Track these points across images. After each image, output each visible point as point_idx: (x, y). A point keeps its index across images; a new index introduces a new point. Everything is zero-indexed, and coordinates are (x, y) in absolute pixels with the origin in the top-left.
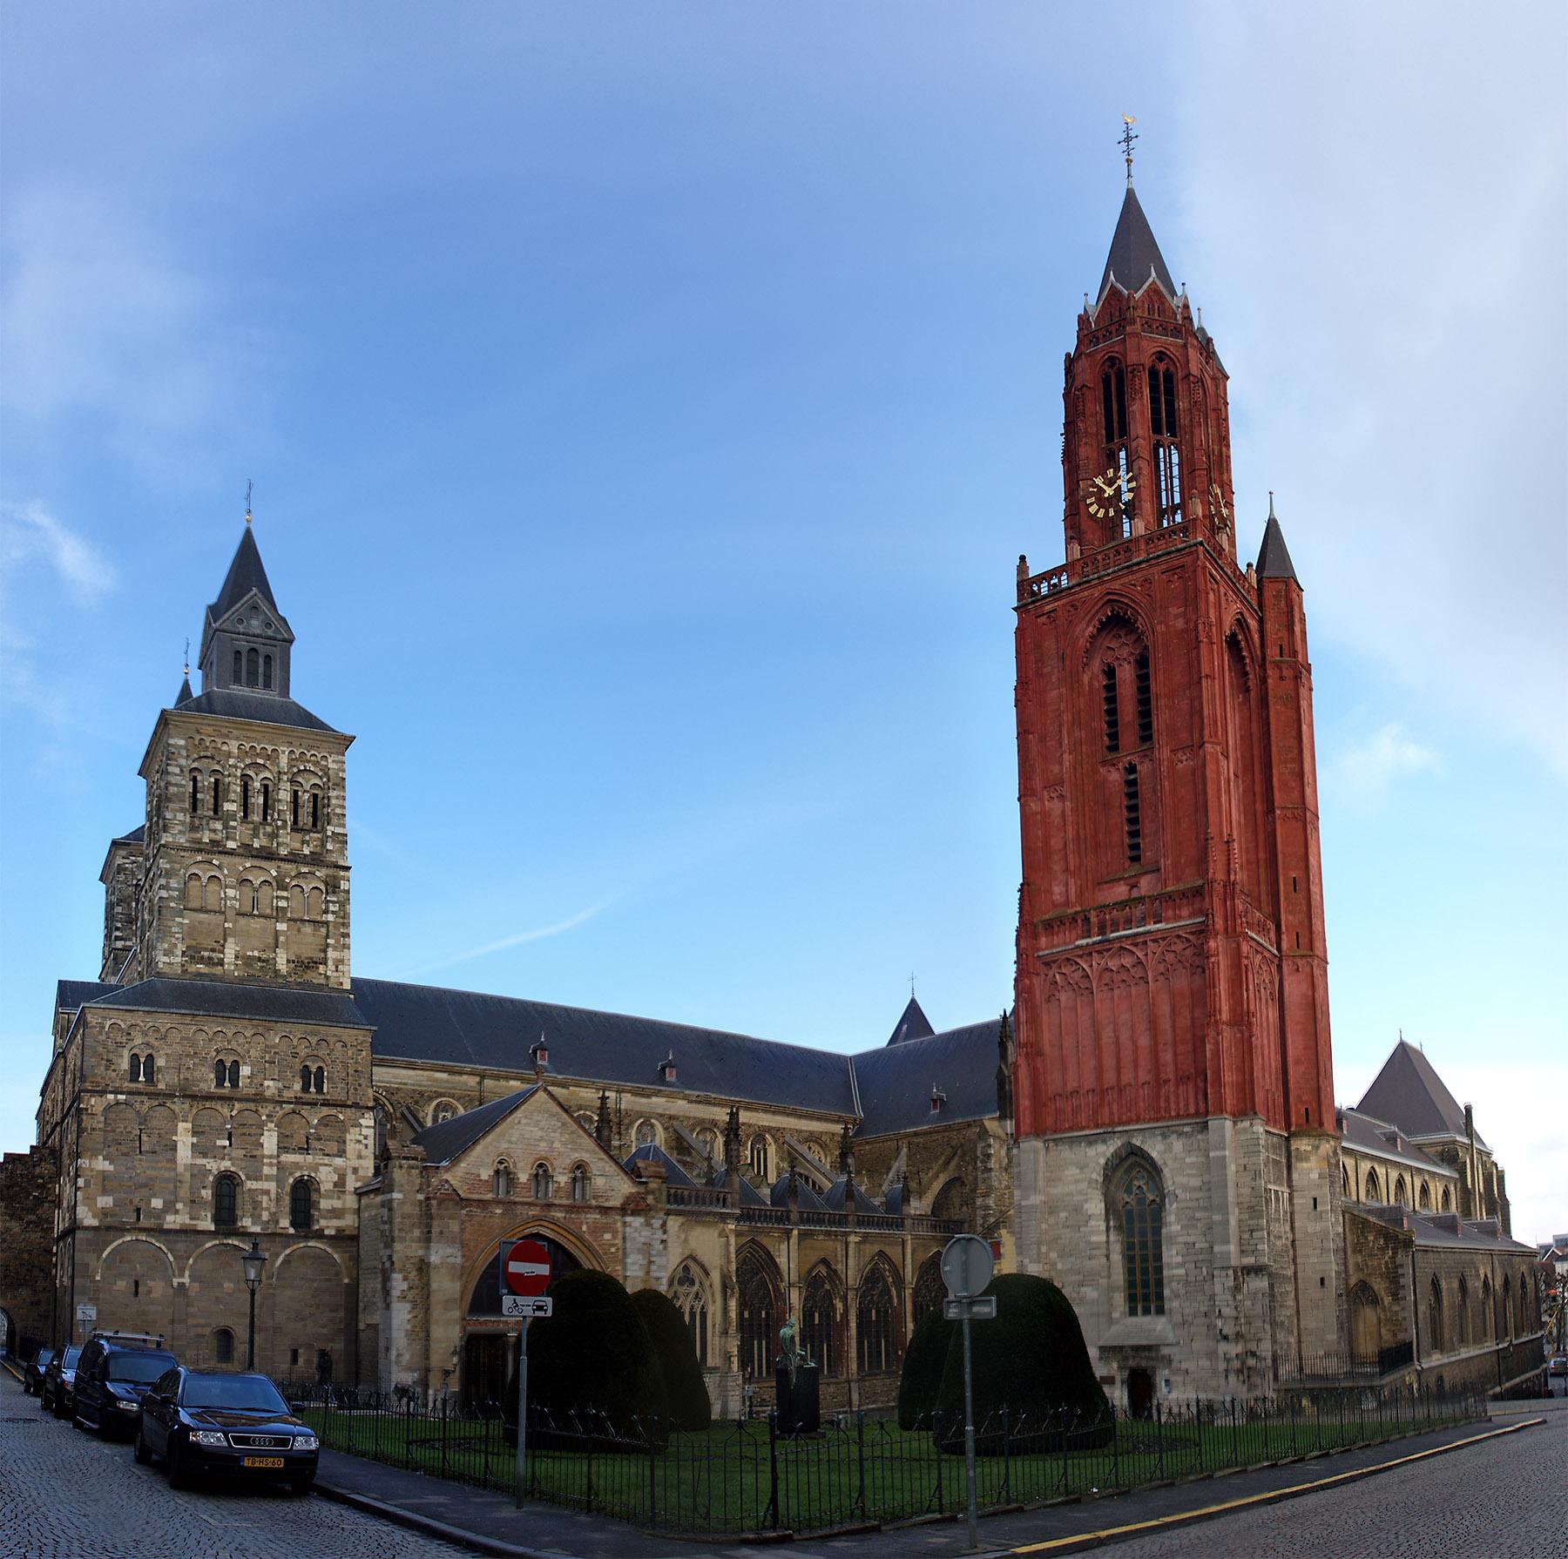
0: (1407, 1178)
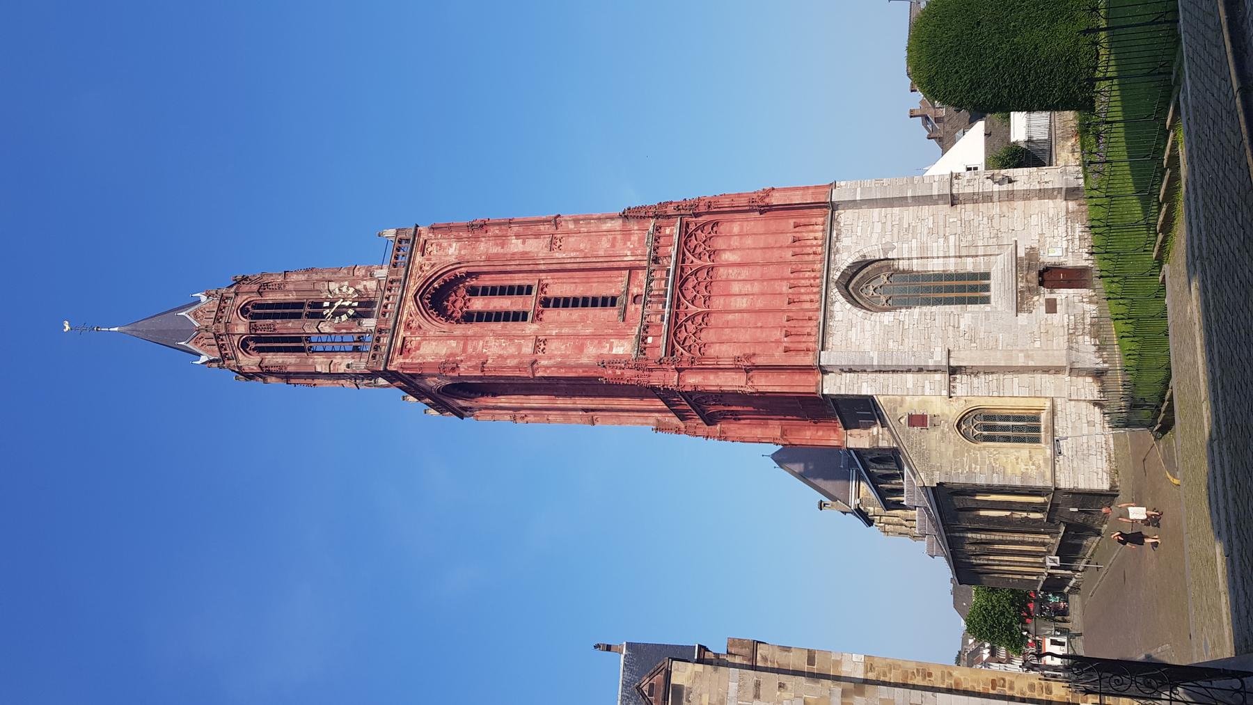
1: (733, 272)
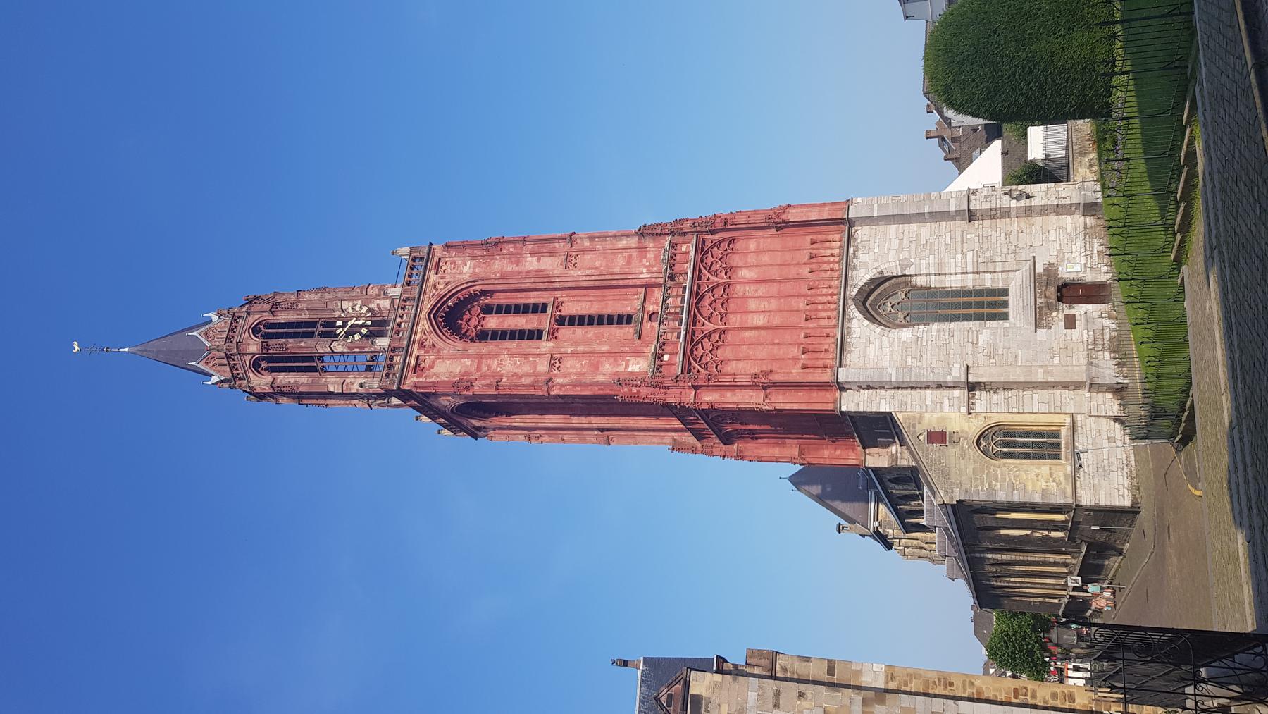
1: (749, 289)
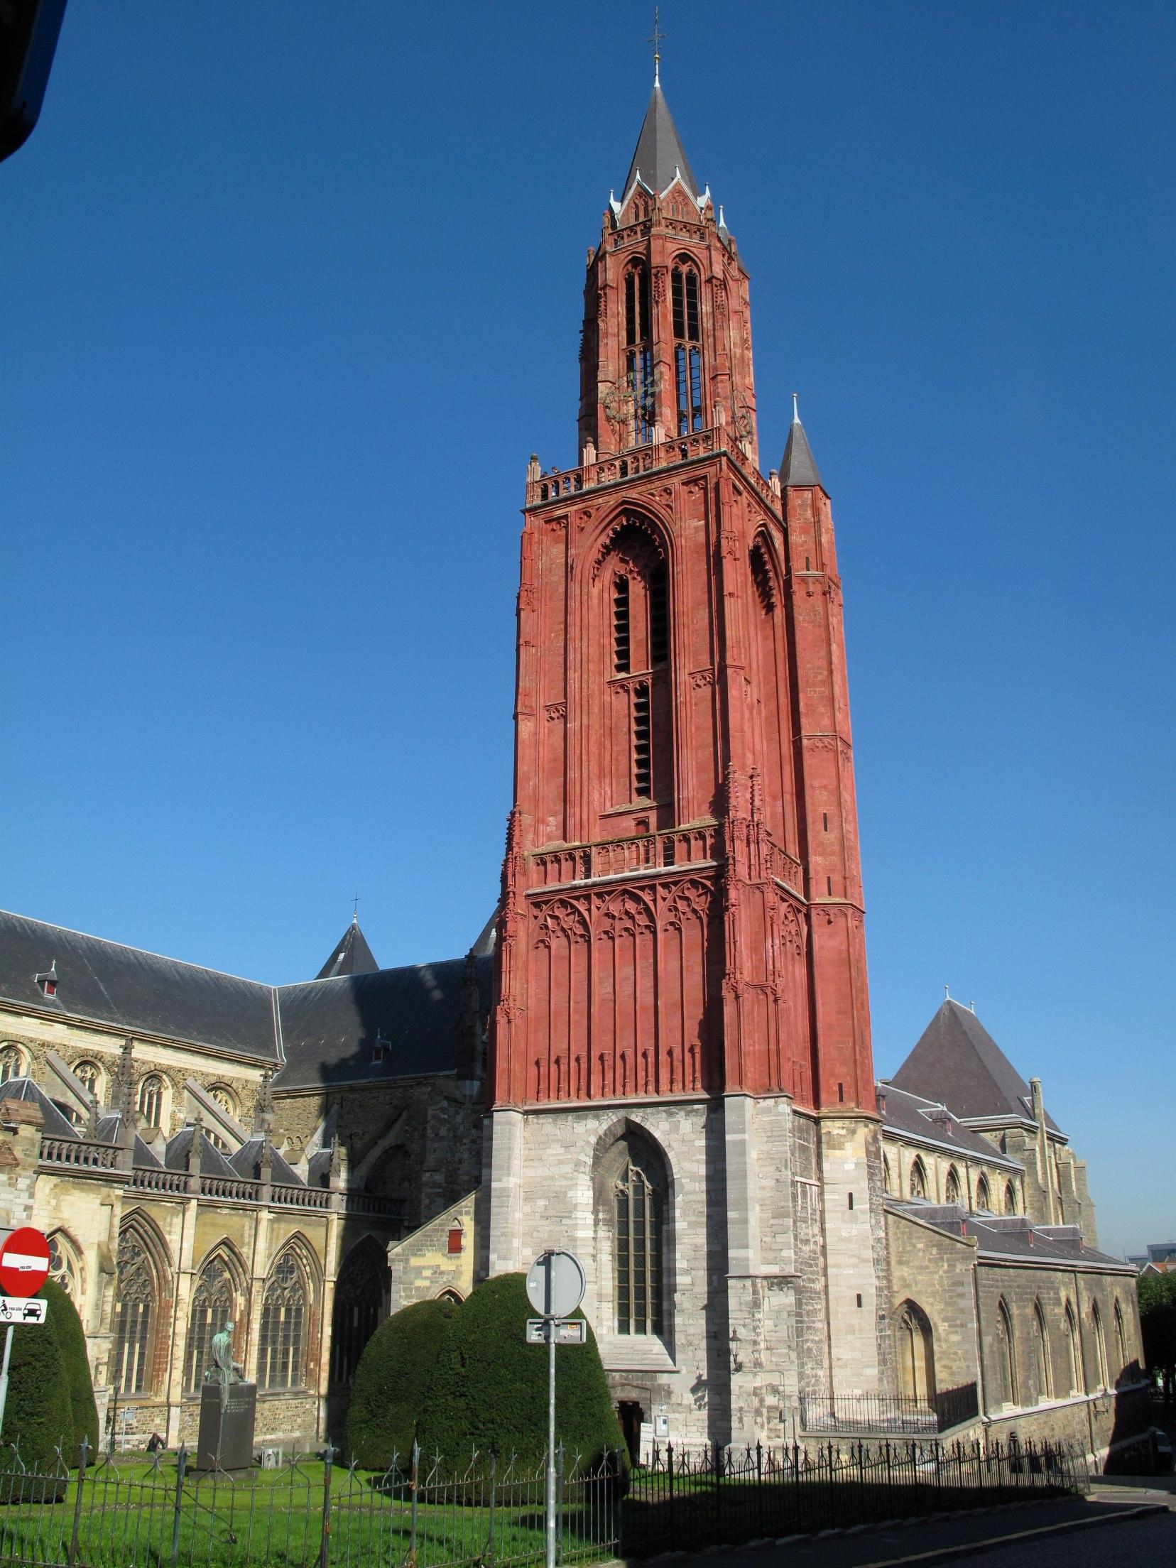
0: (961, 1170)
1: (644, 966)
